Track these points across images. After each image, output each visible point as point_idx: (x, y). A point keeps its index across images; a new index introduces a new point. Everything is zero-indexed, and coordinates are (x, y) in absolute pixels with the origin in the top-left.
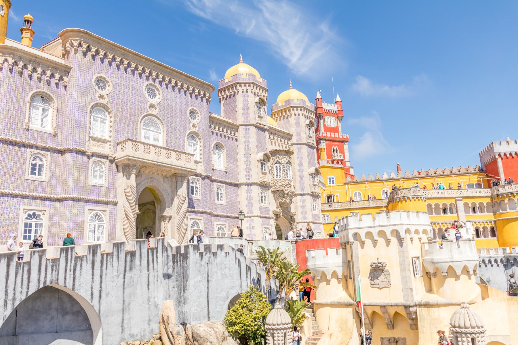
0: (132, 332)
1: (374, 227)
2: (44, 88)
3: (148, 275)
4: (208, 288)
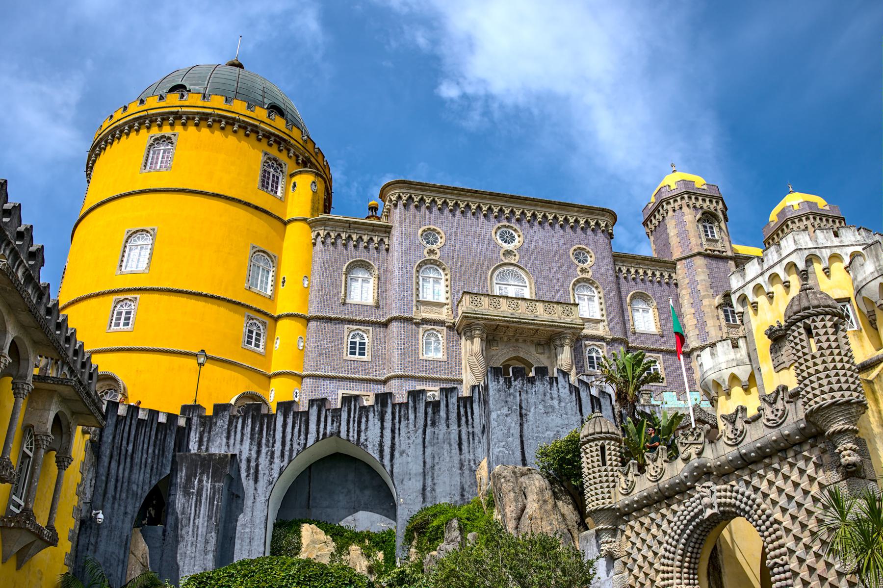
1: (762, 274)
3: (460, 431)
4: (521, 425)
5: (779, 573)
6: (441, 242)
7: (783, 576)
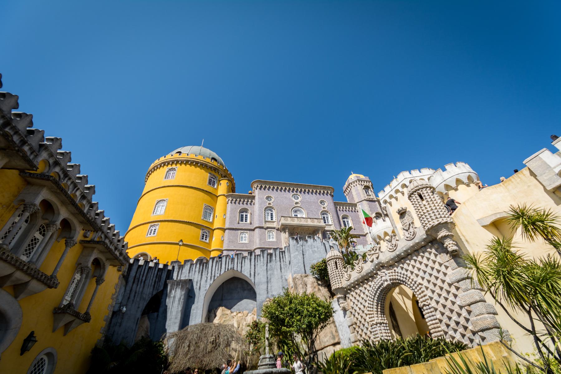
0: (273, 293)
2: (245, 206)
5: (427, 309)
6: (273, 200)
7: (429, 311)
